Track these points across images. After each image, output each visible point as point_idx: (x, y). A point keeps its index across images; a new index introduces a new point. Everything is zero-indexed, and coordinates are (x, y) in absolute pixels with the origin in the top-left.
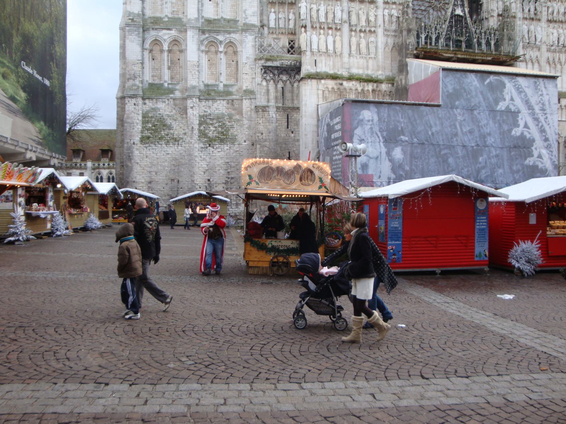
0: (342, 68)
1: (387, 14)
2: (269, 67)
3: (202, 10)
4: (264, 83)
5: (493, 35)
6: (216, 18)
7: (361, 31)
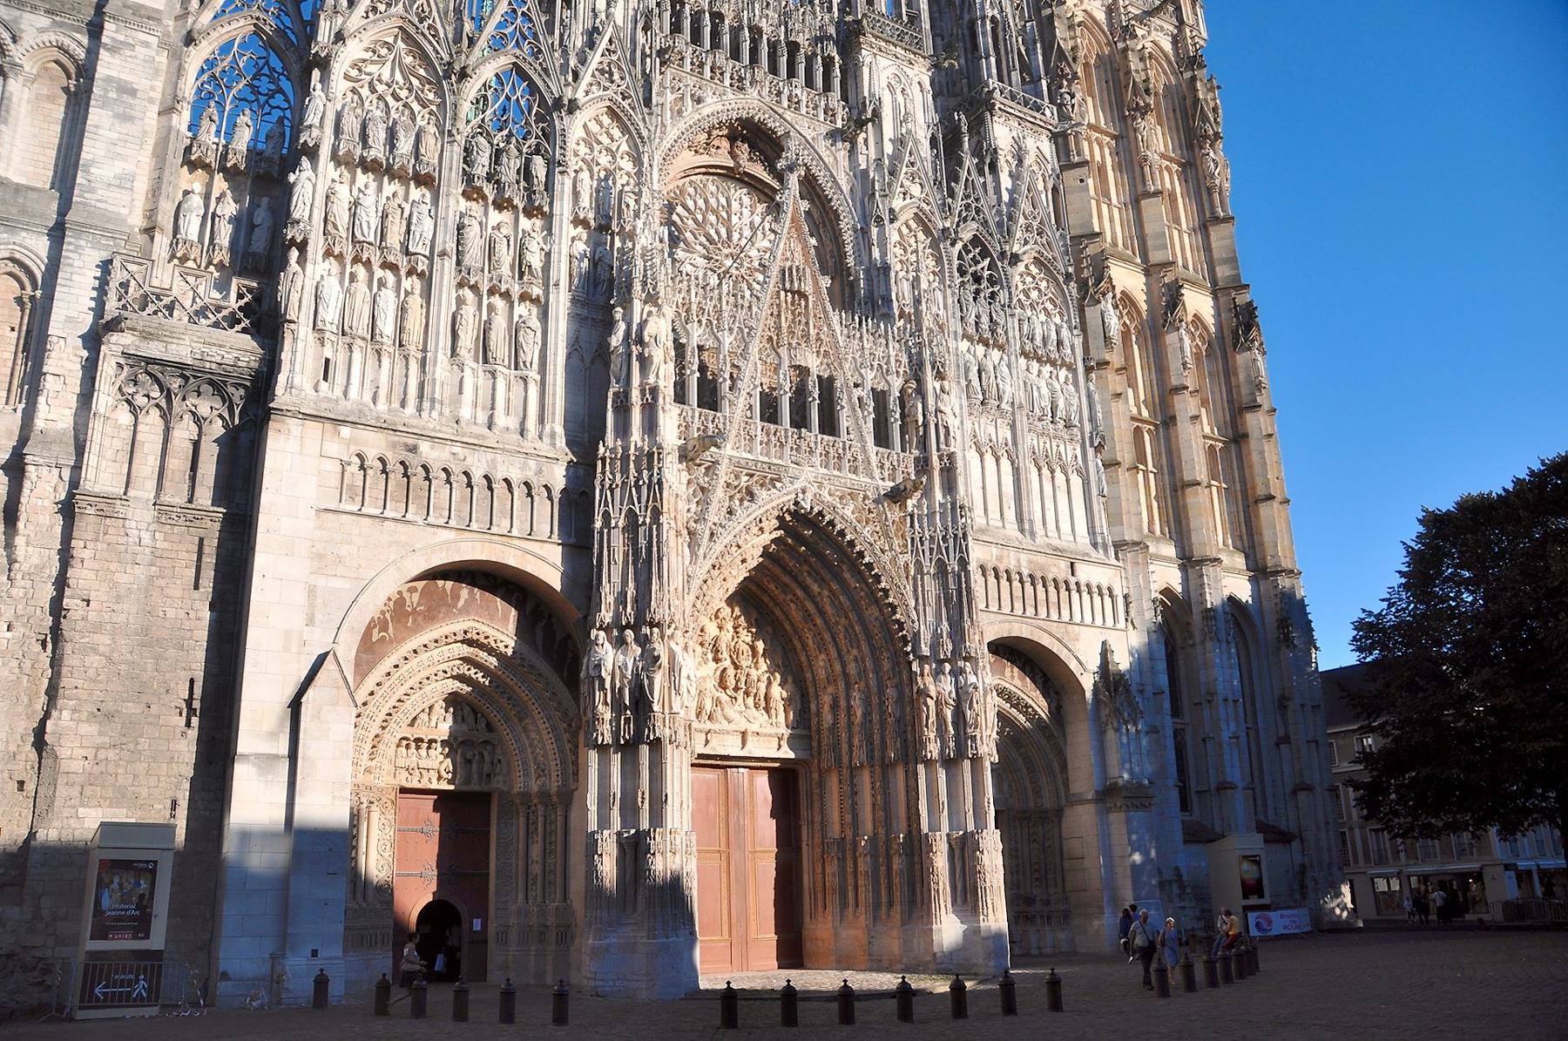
2: (150, 361)
4: (125, 417)
7: (491, 292)
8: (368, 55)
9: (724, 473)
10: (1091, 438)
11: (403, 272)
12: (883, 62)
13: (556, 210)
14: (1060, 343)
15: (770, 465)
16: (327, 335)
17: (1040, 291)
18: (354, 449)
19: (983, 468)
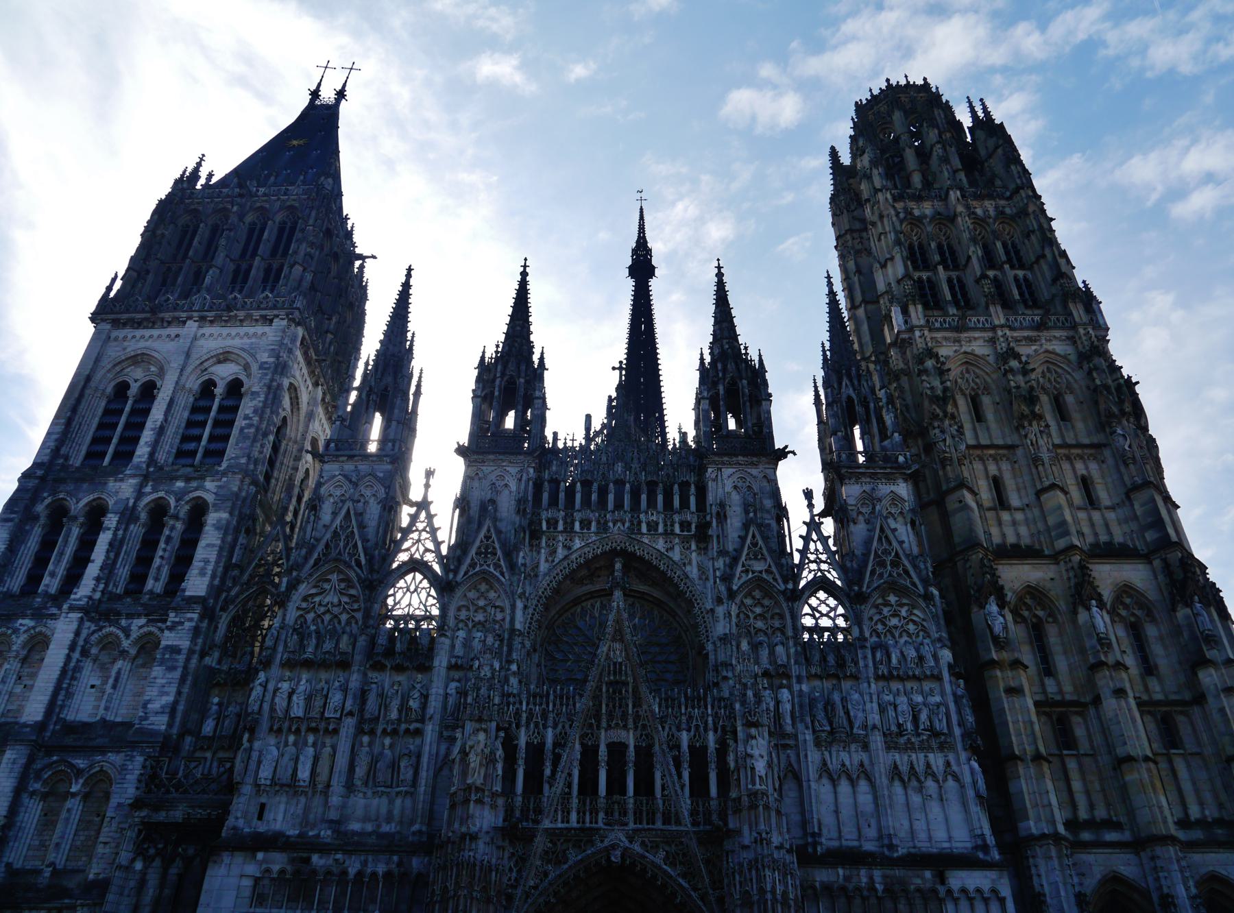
0: (323, 821)
1: (453, 691)
3: (62, 707)
4: (139, 865)
5: (710, 719)
6: (93, 720)
7: (384, 731)
8: (313, 591)
9: (540, 843)
10: (963, 741)
11: (321, 733)
12: (727, 471)
13: (436, 663)
14: (921, 658)
15: (582, 830)
16: (262, 788)
17: (899, 615)
18: (264, 866)
19: (835, 793)
